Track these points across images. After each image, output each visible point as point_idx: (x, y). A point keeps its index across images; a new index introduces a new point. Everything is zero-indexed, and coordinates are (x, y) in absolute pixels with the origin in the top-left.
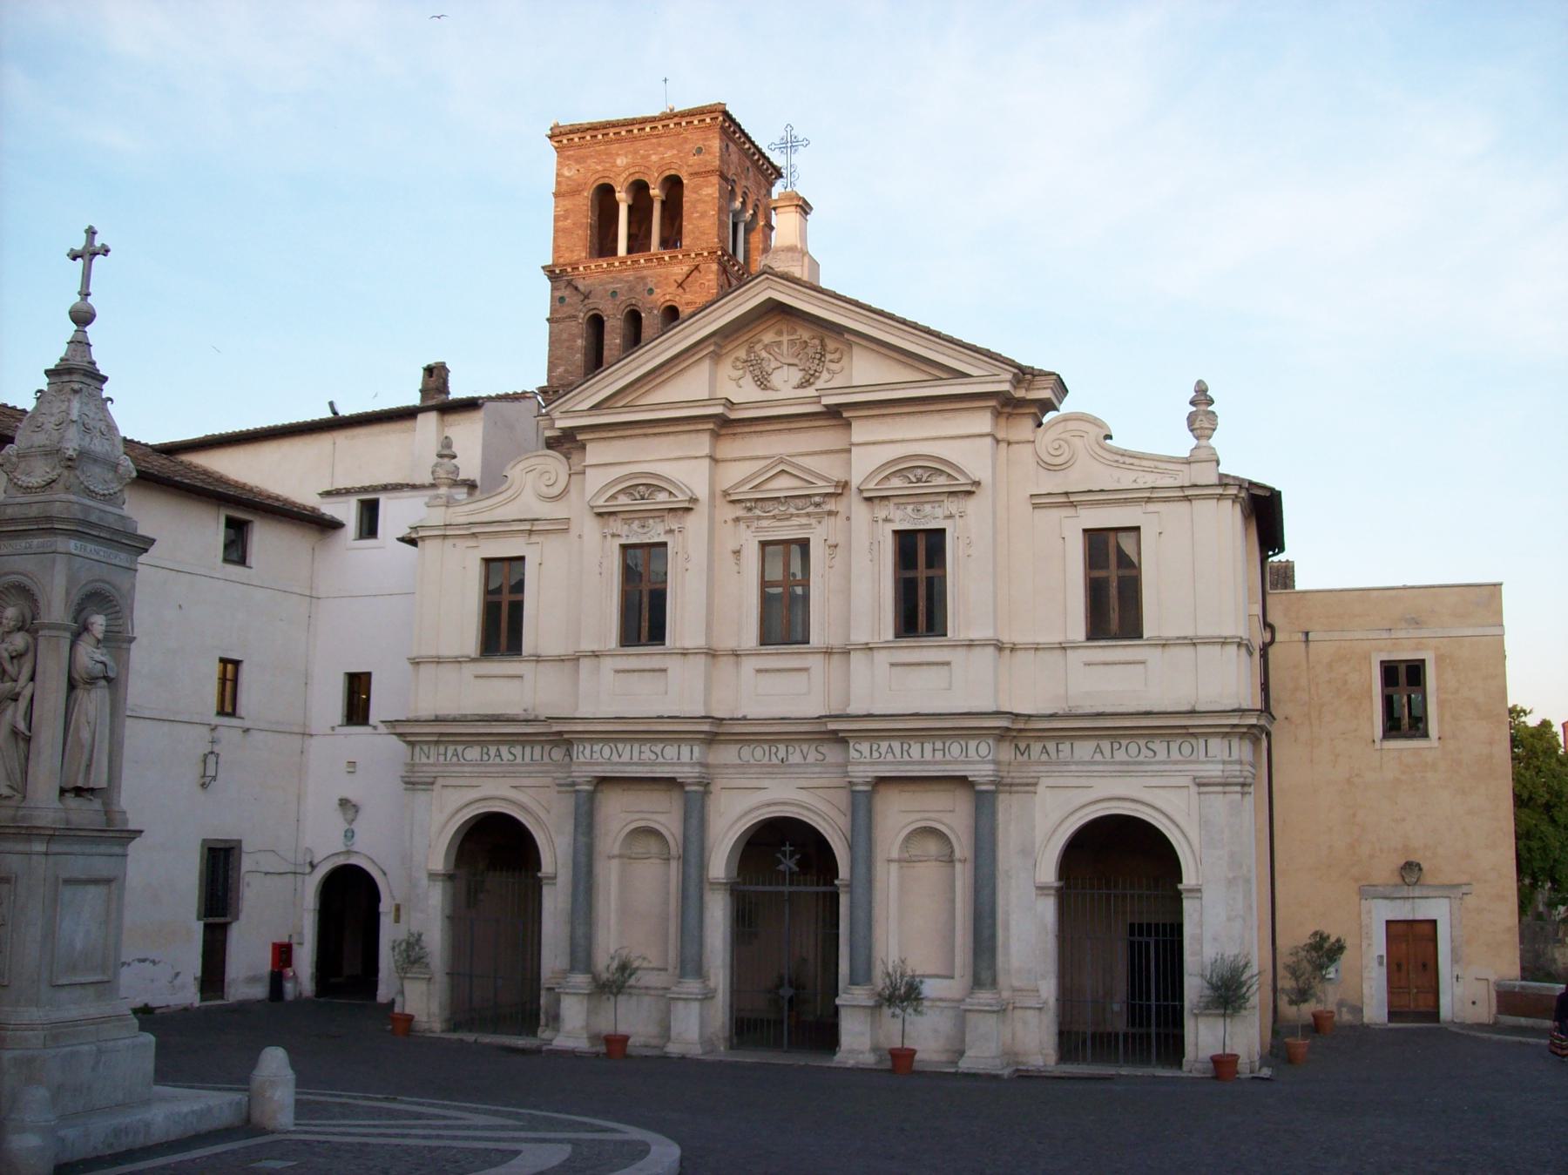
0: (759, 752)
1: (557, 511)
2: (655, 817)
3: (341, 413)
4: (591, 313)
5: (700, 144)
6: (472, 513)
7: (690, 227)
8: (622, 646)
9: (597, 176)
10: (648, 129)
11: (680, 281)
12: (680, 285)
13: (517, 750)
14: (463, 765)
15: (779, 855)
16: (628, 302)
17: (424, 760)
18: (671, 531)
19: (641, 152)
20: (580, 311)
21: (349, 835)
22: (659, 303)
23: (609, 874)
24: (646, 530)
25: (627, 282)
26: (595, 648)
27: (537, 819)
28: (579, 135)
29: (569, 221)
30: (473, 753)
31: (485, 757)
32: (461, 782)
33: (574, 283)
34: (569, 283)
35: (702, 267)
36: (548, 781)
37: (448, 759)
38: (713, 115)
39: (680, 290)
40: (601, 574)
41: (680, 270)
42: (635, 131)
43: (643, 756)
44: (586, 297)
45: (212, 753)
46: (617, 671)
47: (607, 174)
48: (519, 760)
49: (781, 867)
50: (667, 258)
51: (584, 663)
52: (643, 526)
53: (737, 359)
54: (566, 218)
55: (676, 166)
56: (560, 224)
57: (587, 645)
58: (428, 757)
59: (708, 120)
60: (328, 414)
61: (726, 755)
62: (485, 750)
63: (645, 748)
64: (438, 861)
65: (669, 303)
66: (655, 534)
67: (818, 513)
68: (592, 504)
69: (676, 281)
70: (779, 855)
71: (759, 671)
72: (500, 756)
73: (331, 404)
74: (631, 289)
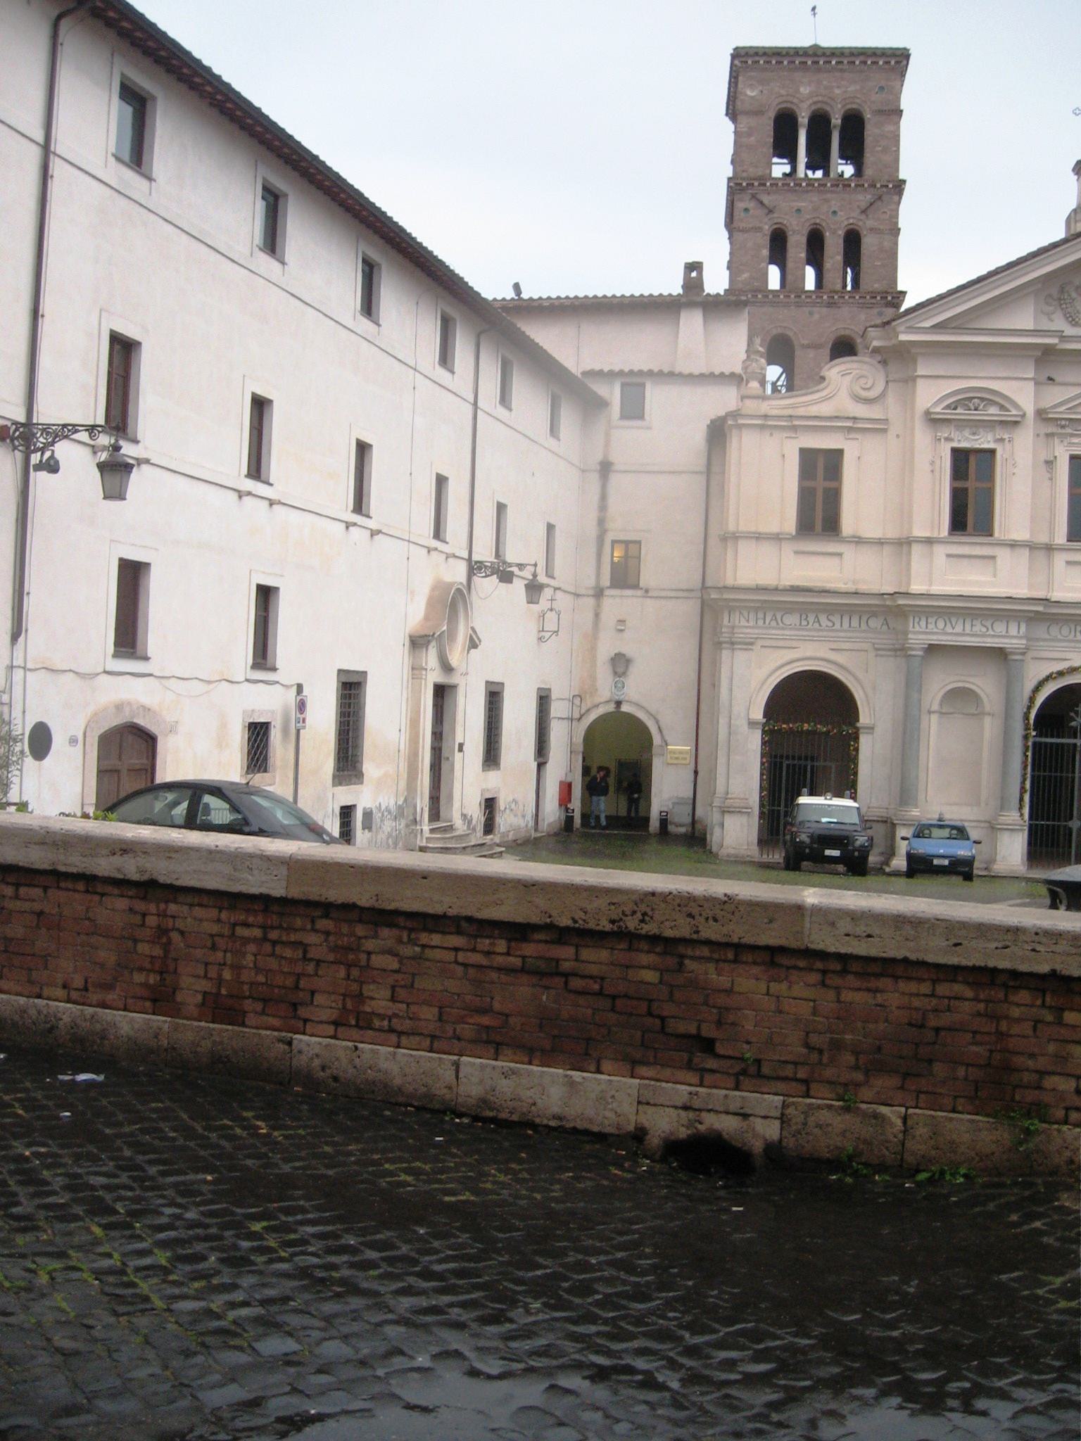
0: (1065, 631)
1: (874, 412)
2: (971, 680)
3: (525, 296)
4: (775, 226)
5: (883, 83)
6: (793, 407)
7: (872, 159)
8: (1068, 541)
9: (781, 99)
10: (834, 62)
11: (863, 208)
12: (864, 212)
13: (836, 619)
14: (783, 629)
15: (1072, 714)
16: (812, 221)
17: (743, 623)
18: (1002, 440)
19: (825, 83)
20: (766, 224)
21: (619, 686)
22: (843, 225)
23: (933, 727)
24: (977, 437)
25: (811, 202)
26: (928, 534)
27: (856, 678)
28: (765, 58)
29: (753, 138)
30: (792, 619)
31: (804, 623)
32: (781, 643)
33: (758, 196)
34: (754, 197)
35: (884, 198)
36: (865, 646)
37: (767, 622)
38: (898, 59)
39: (863, 217)
40: (932, 471)
41: (864, 198)
42: (821, 62)
43: (975, 629)
44: (770, 211)
45: (551, 610)
46: (949, 556)
47: (790, 99)
48: (837, 626)
49: (1073, 724)
50: (853, 185)
51: (917, 550)
52: (974, 434)
53: (1050, 296)
54: (749, 135)
55: (858, 101)
56: (744, 140)
57: (919, 532)
58: (748, 621)
59: (893, 63)
60: (510, 294)
61: (1041, 631)
62: (804, 617)
63: (976, 622)
64: (758, 714)
65: (851, 227)
66: (984, 441)
67: (1060, 434)
68: (932, 410)
69: (858, 207)
70: (1072, 714)
71: (1068, 563)
72: (819, 621)
73: (517, 287)
74: (815, 209)
